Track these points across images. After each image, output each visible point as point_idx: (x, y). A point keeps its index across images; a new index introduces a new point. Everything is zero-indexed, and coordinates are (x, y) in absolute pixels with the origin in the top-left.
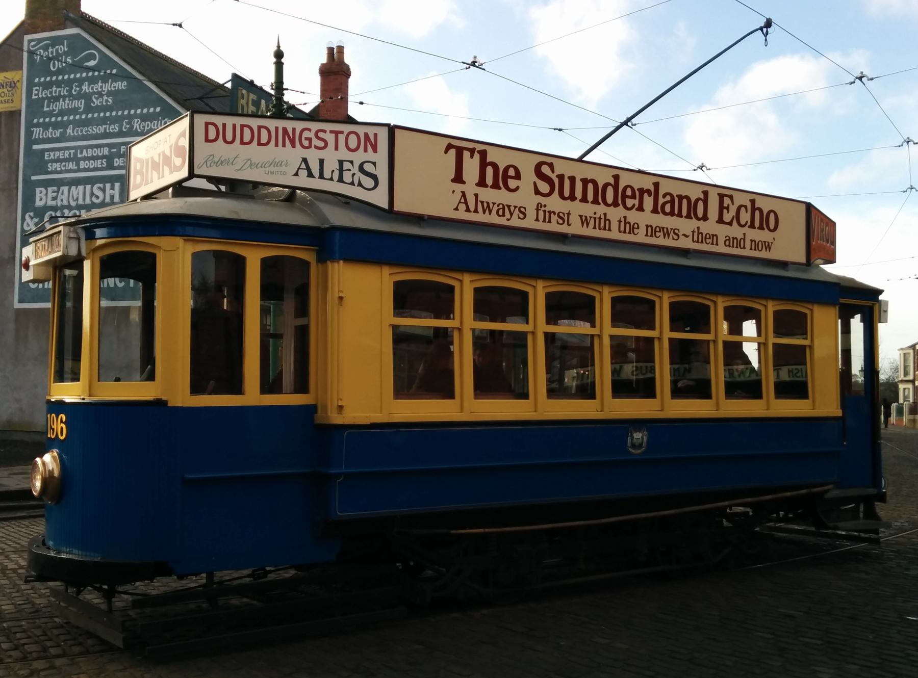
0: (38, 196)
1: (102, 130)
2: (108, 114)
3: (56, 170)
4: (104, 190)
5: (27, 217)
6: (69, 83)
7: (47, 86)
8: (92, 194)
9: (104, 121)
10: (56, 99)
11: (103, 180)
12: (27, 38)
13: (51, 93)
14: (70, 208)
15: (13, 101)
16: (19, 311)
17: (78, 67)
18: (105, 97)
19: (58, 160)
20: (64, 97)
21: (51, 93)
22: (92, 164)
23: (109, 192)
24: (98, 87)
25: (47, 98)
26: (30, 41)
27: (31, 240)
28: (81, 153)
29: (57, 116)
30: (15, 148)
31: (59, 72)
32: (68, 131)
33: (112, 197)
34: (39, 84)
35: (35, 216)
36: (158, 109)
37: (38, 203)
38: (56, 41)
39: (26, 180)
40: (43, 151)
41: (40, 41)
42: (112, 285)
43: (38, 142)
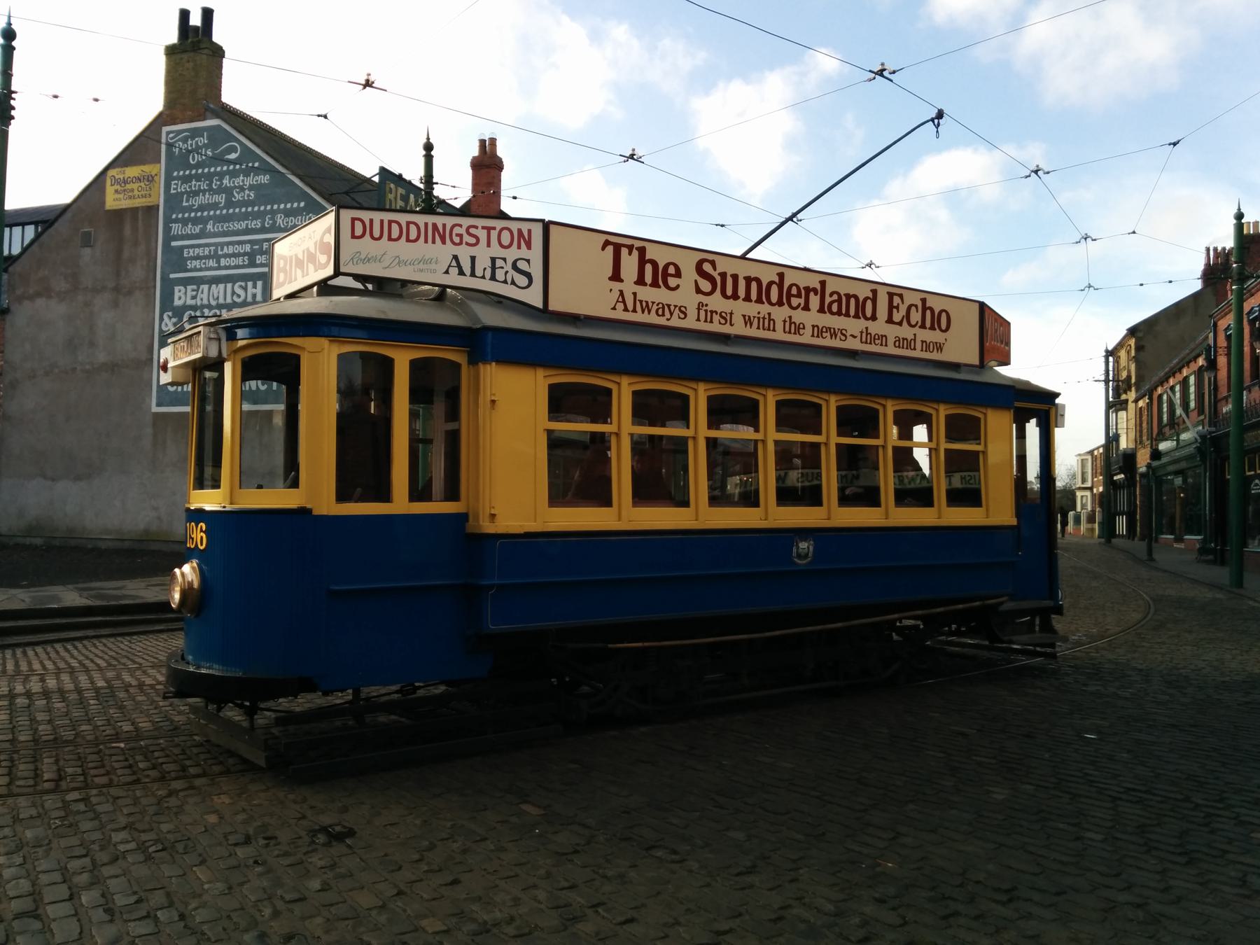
0: (177, 295)
1: (244, 226)
2: (250, 209)
3: (196, 268)
4: (245, 289)
5: (165, 317)
6: (209, 177)
7: (186, 179)
8: (233, 293)
9: (245, 216)
10: (196, 193)
12: (165, 129)
14: (210, 307)
16: (156, 414)
17: (219, 159)
20: (204, 192)
22: (233, 262)
23: (250, 290)
24: (239, 181)
26: (168, 133)
27: (170, 341)
29: (196, 211)
30: (153, 244)
31: (198, 165)
33: (254, 296)
34: (178, 178)
35: (174, 316)
36: (302, 204)
37: (177, 303)
38: (195, 133)
39: (165, 279)
40: (183, 247)
41: (179, 132)
42: (254, 388)
43: (177, 238)
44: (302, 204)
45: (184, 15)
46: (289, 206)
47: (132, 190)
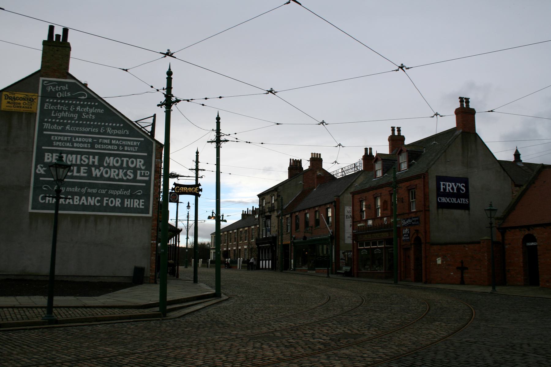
1: (88, 130)
2: (92, 123)
4: (89, 159)
6: (69, 105)
8: (81, 160)
9: (89, 126)
11: (89, 154)
12: (41, 79)
13: (57, 108)
15: (31, 108)
17: (75, 98)
18: (90, 115)
19: (60, 141)
20: (65, 111)
21: (57, 108)
22: (81, 145)
25: (54, 110)
26: (43, 81)
28: (75, 139)
29: (60, 119)
31: (62, 98)
32: (67, 128)
33: (94, 162)
34: (49, 102)
36: (122, 125)
39: (38, 148)
40: (51, 135)
42: (92, 204)
44: (122, 125)
45: (51, 28)
46: (114, 125)
47: (20, 104)
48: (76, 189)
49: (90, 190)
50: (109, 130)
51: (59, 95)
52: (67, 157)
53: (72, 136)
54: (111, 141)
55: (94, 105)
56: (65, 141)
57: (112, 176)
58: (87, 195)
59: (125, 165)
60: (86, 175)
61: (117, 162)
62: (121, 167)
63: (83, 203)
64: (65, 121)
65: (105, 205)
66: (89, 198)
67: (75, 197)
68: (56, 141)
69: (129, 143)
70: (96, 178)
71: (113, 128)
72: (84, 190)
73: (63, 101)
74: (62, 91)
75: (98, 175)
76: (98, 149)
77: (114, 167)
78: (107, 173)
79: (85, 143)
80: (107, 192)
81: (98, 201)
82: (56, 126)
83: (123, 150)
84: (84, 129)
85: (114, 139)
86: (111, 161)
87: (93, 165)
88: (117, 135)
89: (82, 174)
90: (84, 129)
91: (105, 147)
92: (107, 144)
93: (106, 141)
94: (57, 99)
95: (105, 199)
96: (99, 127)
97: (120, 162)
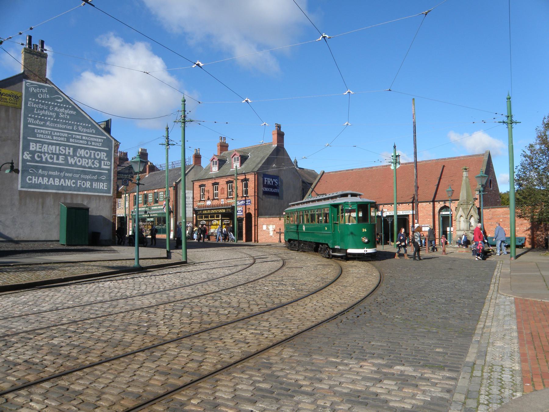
1: (64, 127)
4: (65, 149)
5: (25, 153)
7: (35, 103)
8: (60, 150)
9: (65, 124)
10: (42, 109)
14: (48, 153)
16: (20, 191)
19: (42, 134)
20: (45, 110)
22: (60, 139)
23: (67, 150)
24: (62, 110)
31: (42, 99)
37: (31, 149)
38: (41, 87)
40: (34, 128)
41: (32, 84)
48: (56, 173)
49: (67, 175)
50: (80, 128)
51: (40, 96)
52: (48, 147)
53: (51, 131)
54: (82, 137)
55: (69, 108)
56: (46, 134)
57: (83, 165)
58: (65, 178)
59: (92, 157)
60: (63, 162)
61: (87, 153)
62: (90, 158)
63: (62, 184)
64: (46, 118)
65: (78, 186)
66: (67, 180)
67: (56, 179)
68: (39, 133)
69: (95, 140)
70: (71, 165)
71: (83, 127)
72: (62, 174)
73: (43, 102)
74: (42, 93)
75: (73, 163)
76: (72, 142)
77: (85, 157)
78: (79, 161)
79: (62, 137)
80: (80, 176)
81: (74, 183)
82: (38, 121)
83: (91, 145)
84: (61, 126)
85: (84, 136)
86: (82, 152)
87: (69, 155)
88: (86, 133)
89: (60, 162)
90: (61, 126)
91: (77, 141)
92: (78, 139)
93: (78, 137)
94: (39, 99)
95: (79, 181)
96: (73, 125)
97: (89, 154)
